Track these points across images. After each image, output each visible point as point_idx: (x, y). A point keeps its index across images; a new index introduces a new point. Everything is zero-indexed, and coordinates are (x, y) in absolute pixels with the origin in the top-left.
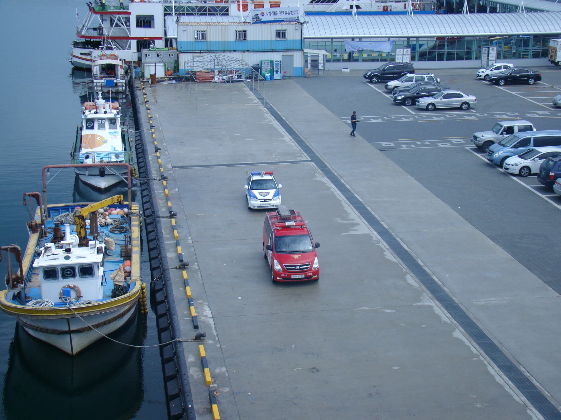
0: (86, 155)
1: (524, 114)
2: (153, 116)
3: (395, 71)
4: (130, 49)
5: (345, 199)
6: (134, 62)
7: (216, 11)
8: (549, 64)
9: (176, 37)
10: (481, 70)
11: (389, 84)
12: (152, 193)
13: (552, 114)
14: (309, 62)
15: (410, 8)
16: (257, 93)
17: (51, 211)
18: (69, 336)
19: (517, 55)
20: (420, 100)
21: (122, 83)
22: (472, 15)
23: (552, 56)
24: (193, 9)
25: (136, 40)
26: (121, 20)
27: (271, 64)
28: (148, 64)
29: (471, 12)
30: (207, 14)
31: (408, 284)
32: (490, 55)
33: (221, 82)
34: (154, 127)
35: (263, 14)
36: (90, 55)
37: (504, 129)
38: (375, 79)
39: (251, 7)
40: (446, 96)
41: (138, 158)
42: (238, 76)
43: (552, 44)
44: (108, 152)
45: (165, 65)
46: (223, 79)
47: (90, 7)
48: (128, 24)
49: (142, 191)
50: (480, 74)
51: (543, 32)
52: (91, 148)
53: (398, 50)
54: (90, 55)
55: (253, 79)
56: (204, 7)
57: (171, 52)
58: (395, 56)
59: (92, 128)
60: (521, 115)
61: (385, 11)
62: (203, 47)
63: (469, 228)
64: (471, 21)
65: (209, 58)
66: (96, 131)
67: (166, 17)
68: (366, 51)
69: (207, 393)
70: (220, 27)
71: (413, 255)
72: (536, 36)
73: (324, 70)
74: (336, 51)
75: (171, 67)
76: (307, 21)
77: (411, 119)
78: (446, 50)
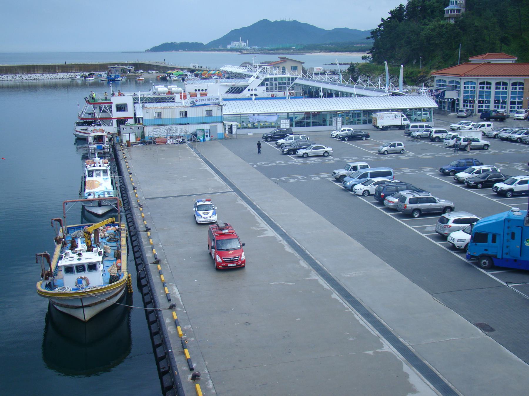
1: (362, 158)
2: (130, 167)
3: (281, 133)
4: (112, 125)
5: (257, 215)
6: (116, 133)
7: (167, 100)
8: (373, 127)
10: (333, 132)
11: (278, 141)
12: (133, 215)
13: (378, 157)
14: (227, 129)
15: (288, 95)
16: (195, 150)
17: (69, 230)
18: (82, 309)
19: (354, 123)
20: (298, 151)
21: (107, 147)
22: (325, 99)
23: (374, 123)
24: (152, 99)
29: (325, 97)
31: (301, 266)
32: (338, 123)
33: (172, 144)
37: (352, 167)
38: (269, 139)
39: (188, 96)
40: (314, 149)
41: (122, 194)
42: (183, 140)
43: (374, 115)
44: (103, 191)
45: (136, 135)
46: (173, 142)
47: (86, 100)
48: (111, 110)
49: (126, 215)
50: (333, 134)
51: (368, 109)
53: (282, 121)
58: (280, 124)
60: (360, 158)
61: (273, 97)
62: (160, 122)
63: (336, 229)
64: (325, 102)
65: (164, 129)
66: (94, 178)
67: (135, 104)
68: (263, 122)
69: (181, 342)
71: (303, 248)
72: (364, 111)
73: (237, 134)
74: (243, 122)
75: (140, 135)
76: (225, 104)
77: (294, 163)
78: (311, 120)
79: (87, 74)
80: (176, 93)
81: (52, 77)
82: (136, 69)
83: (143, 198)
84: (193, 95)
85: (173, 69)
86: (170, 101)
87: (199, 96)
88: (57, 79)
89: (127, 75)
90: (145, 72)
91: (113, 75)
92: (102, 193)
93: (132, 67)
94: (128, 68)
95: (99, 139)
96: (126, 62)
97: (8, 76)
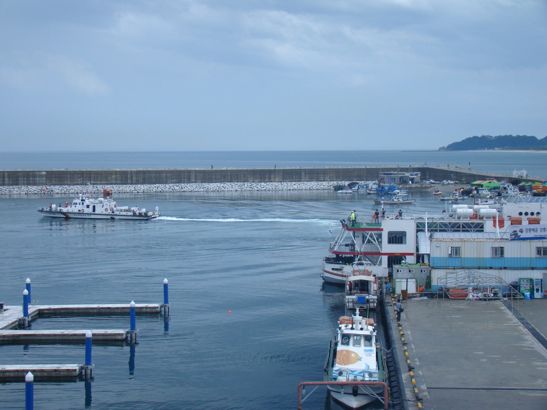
0: (339, 371)
2: (405, 333)
4: (381, 265)
6: (386, 278)
7: (470, 227)
9: (429, 252)
16: (516, 313)
24: (445, 225)
25: (388, 256)
26: (373, 236)
27: (530, 282)
28: (399, 280)
30: (461, 231)
33: (476, 300)
34: (406, 345)
35: (521, 231)
36: (341, 270)
39: (507, 223)
42: (494, 294)
45: (417, 281)
46: (478, 297)
47: (343, 224)
48: (380, 240)
52: (345, 365)
54: (341, 270)
55: (512, 298)
56: (459, 223)
57: (423, 268)
59: (348, 344)
62: (457, 263)
65: (463, 275)
67: (419, 233)
70: (475, 243)
79: (347, 183)
80: (487, 218)
81: (295, 187)
82: (423, 178)
83: (424, 387)
84: (516, 222)
85: (483, 178)
86: (453, 229)
87: (525, 223)
88: (302, 190)
89: (408, 186)
90: (438, 182)
91: (386, 186)
92: (360, 373)
93: (416, 175)
94: (411, 175)
95: (363, 286)
96: (408, 167)
97: (232, 184)
